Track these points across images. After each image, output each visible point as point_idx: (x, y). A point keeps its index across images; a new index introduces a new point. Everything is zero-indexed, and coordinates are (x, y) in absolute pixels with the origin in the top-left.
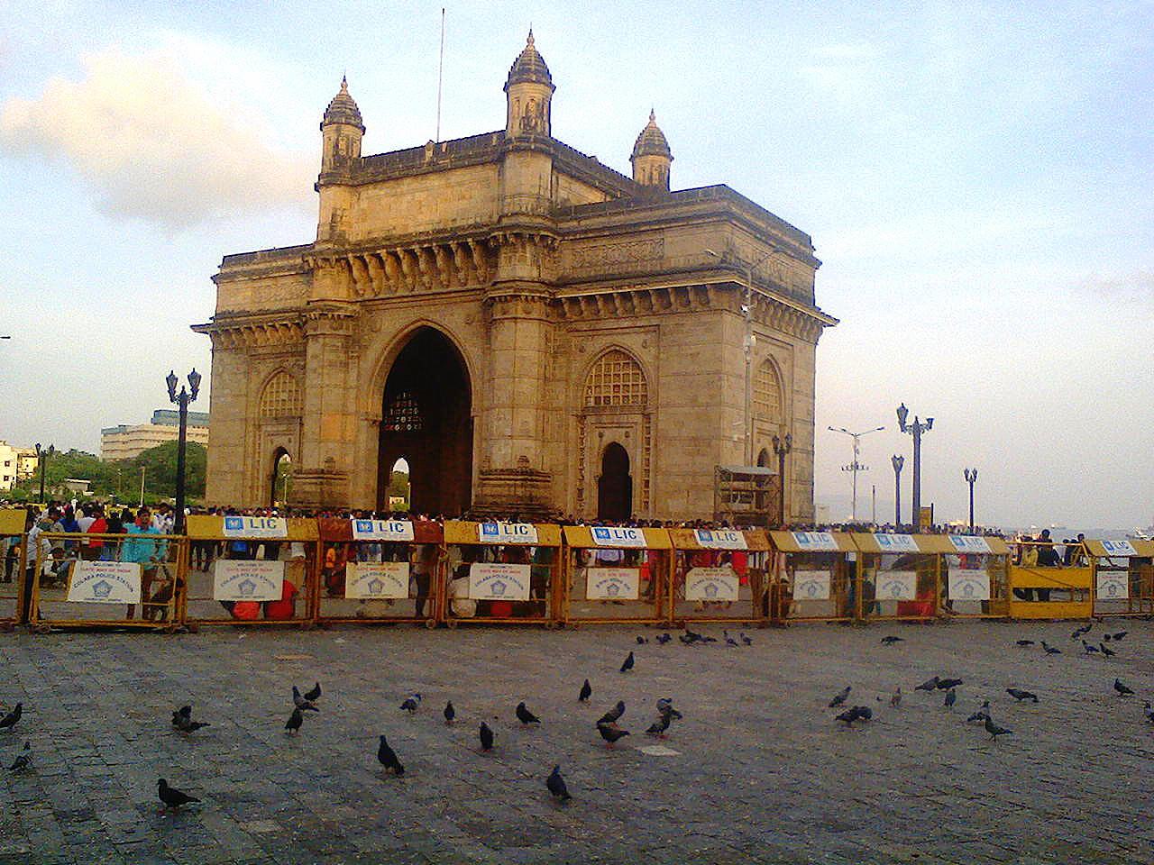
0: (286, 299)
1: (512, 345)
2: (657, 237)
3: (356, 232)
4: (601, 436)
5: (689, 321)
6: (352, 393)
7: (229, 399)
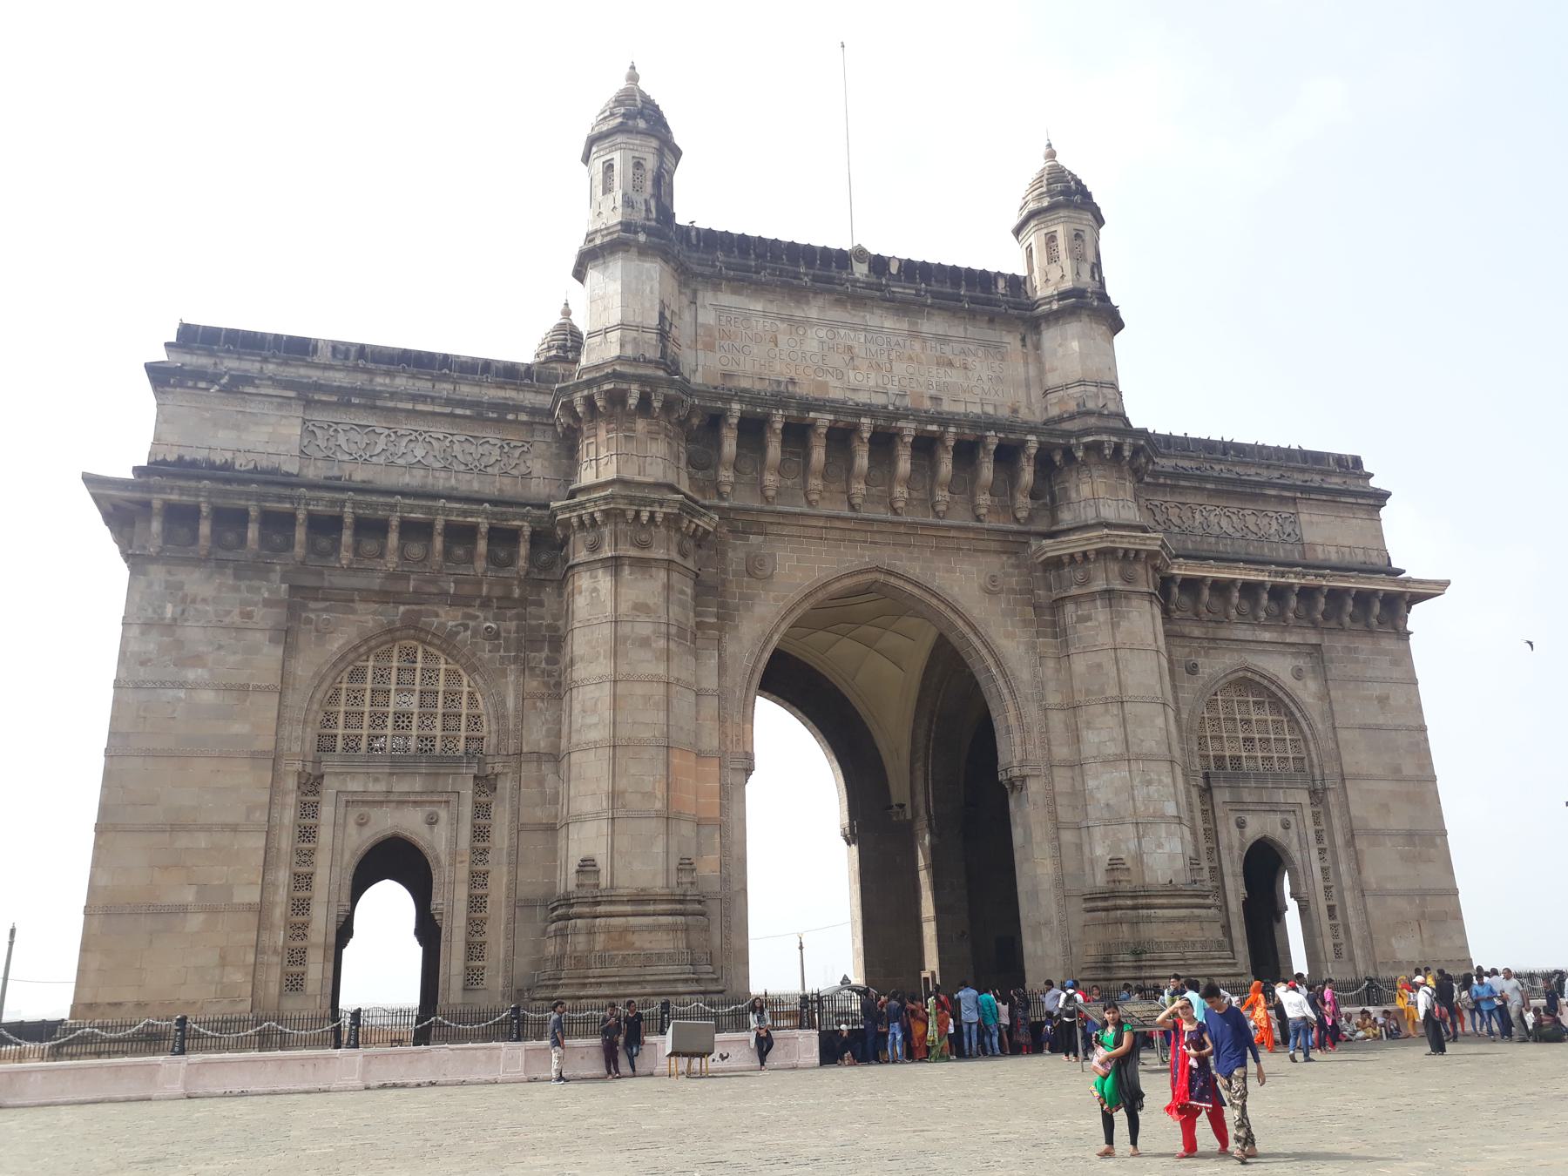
0: (426, 467)
1: (1150, 639)
2: (1287, 510)
3: (701, 368)
4: (1241, 825)
5: (1364, 645)
6: (710, 706)
7: (208, 697)
